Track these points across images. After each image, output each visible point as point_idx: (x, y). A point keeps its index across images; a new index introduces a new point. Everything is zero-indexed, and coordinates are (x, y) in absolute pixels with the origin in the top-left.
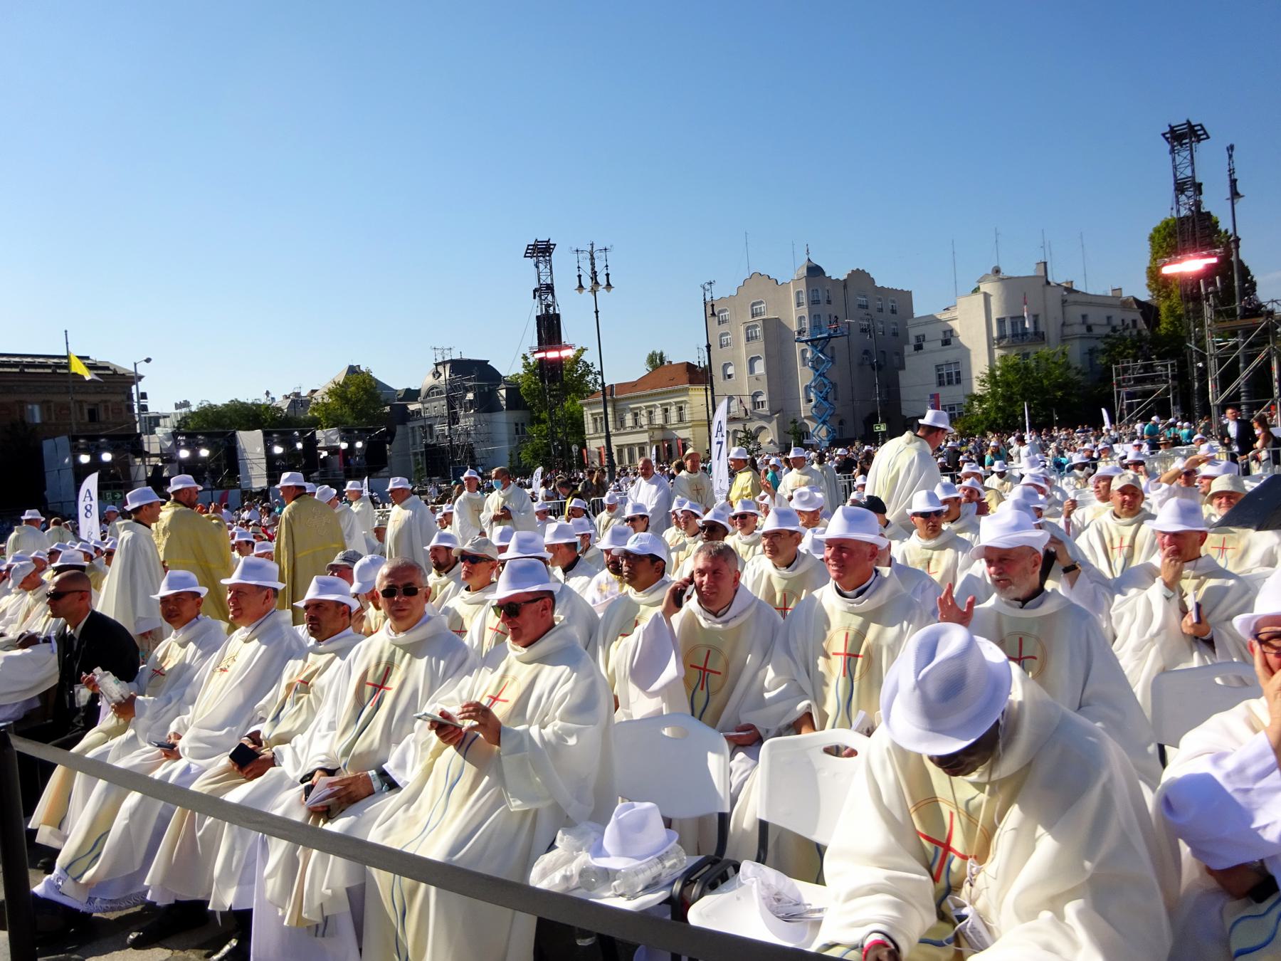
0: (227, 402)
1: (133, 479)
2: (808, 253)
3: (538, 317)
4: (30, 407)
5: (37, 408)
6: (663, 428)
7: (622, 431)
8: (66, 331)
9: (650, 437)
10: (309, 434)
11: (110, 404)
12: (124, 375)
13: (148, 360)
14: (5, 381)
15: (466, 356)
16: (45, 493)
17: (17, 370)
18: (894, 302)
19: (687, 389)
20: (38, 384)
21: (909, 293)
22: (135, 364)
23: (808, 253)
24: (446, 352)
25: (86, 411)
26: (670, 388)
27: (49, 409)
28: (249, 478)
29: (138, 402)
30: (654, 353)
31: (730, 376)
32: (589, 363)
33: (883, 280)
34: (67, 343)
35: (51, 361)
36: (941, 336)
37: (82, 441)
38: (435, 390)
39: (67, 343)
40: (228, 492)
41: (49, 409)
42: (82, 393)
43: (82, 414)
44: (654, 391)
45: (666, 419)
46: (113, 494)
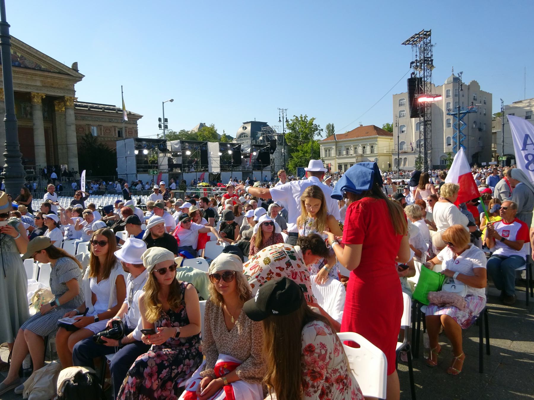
1: (159, 164)
2: (453, 71)
3: (409, 79)
4: (92, 128)
5: (95, 128)
6: (362, 156)
7: (329, 158)
8: (122, 86)
9: (357, 160)
10: (237, 146)
11: (127, 129)
13: (172, 101)
14: (82, 114)
15: (257, 120)
16: (117, 169)
17: (87, 109)
18: (485, 98)
19: (377, 138)
20: (96, 116)
21: (491, 94)
22: (163, 103)
23: (453, 71)
24: (284, 111)
25: (117, 132)
26: (368, 137)
27: (101, 130)
28: (211, 167)
29: (164, 123)
30: (329, 124)
31: (403, 132)
32: (317, 125)
33: (483, 88)
34: (122, 92)
35: (101, 106)
36: (525, 114)
38: (243, 135)
39: (122, 92)
40: (204, 174)
41: (101, 130)
43: (115, 133)
44: (359, 138)
45: (364, 152)
46: (153, 171)
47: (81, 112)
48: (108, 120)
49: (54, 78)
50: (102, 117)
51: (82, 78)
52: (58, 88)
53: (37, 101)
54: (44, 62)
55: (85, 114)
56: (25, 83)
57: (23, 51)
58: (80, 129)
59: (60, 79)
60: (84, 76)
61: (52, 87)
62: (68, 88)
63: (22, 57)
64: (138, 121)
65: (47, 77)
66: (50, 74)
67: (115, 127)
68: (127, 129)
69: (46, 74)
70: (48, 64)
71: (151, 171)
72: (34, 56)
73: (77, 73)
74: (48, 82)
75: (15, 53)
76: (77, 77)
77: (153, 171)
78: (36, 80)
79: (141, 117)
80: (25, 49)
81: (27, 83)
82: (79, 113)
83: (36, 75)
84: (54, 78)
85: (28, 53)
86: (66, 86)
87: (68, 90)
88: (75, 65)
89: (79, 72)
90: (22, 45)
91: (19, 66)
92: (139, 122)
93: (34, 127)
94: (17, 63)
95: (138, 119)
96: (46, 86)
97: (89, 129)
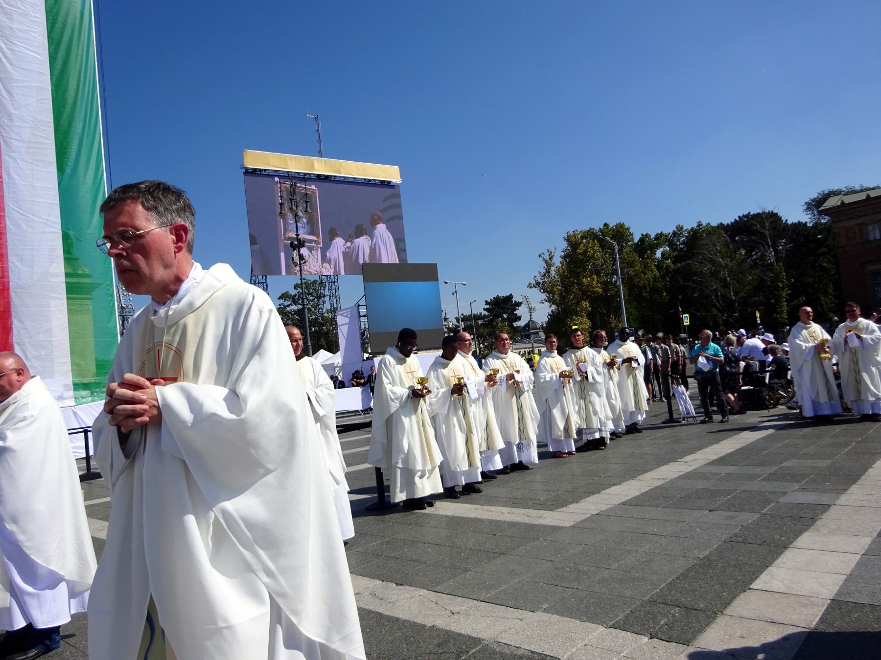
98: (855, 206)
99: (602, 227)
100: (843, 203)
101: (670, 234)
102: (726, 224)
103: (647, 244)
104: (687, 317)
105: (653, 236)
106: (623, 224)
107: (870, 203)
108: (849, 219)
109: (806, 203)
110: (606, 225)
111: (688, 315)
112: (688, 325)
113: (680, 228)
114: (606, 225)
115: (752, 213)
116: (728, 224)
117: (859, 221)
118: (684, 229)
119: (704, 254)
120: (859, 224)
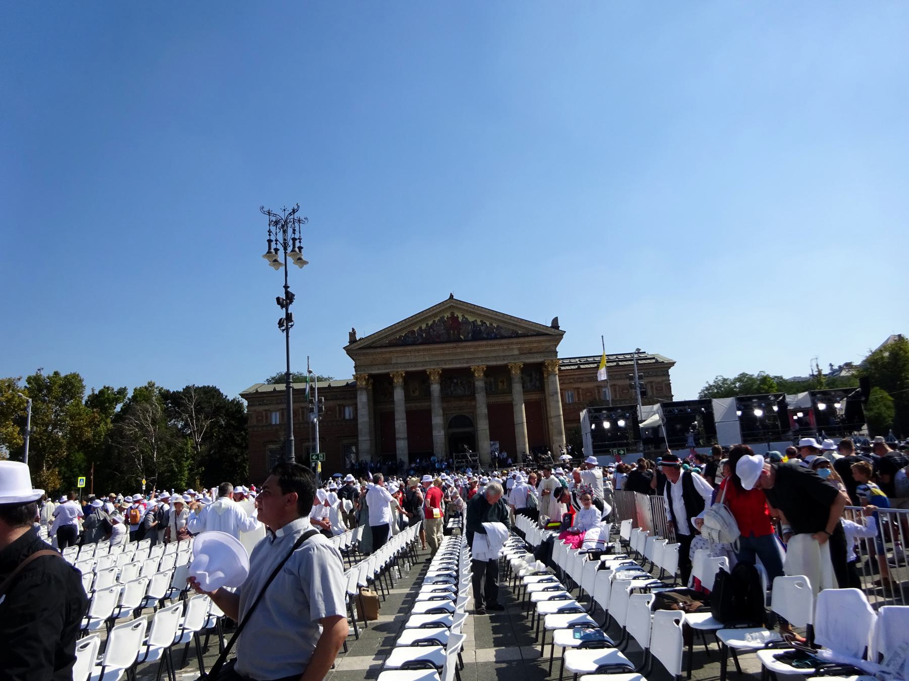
0: (737, 376)
4: (604, 390)
8: (602, 337)
11: (654, 384)
12: (663, 362)
37: (604, 412)
41: (615, 391)
42: (617, 379)
46: (619, 451)
47: (586, 372)
48: (624, 376)
49: (532, 342)
50: (615, 373)
51: (563, 335)
52: (536, 353)
53: (516, 373)
54: (521, 327)
55: (592, 373)
56: (502, 354)
57: (499, 320)
58: (588, 394)
59: (539, 342)
60: (565, 332)
61: (530, 352)
62: (548, 350)
63: (498, 326)
64: (670, 371)
65: (523, 343)
66: (527, 339)
67: (651, 382)
68: (654, 384)
69: (522, 340)
70: (524, 328)
71: (615, 450)
72: (509, 324)
73: (556, 331)
74: (526, 348)
75: (491, 324)
76: (556, 335)
77: (619, 451)
78: (513, 349)
79: (673, 364)
80: (500, 318)
81: (504, 354)
82: (583, 374)
83: (512, 344)
84: (532, 342)
85: (503, 322)
86: (547, 348)
87: (550, 352)
88: (555, 320)
89: (560, 329)
90: (496, 315)
91: (495, 338)
92: (671, 371)
93: (514, 403)
94: (493, 335)
95: (669, 368)
96: (524, 353)
97: (599, 392)
98: (265, 395)
99: (51, 375)
100: (275, 389)
101: (122, 391)
102: (182, 391)
103: (106, 396)
104: (83, 480)
105: (115, 390)
106: (78, 375)
107: (274, 395)
108: (260, 405)
109: (267, 380)
110: (56, 373)
111: (84, 478)
112: (82, 488)
113: (151, 385)
114: (56, 373)
115: (196, 386)
116: (174, 392)
117: (266, 408)
118: (156, 386)
119: (131, 419)
120: (266, 410)
